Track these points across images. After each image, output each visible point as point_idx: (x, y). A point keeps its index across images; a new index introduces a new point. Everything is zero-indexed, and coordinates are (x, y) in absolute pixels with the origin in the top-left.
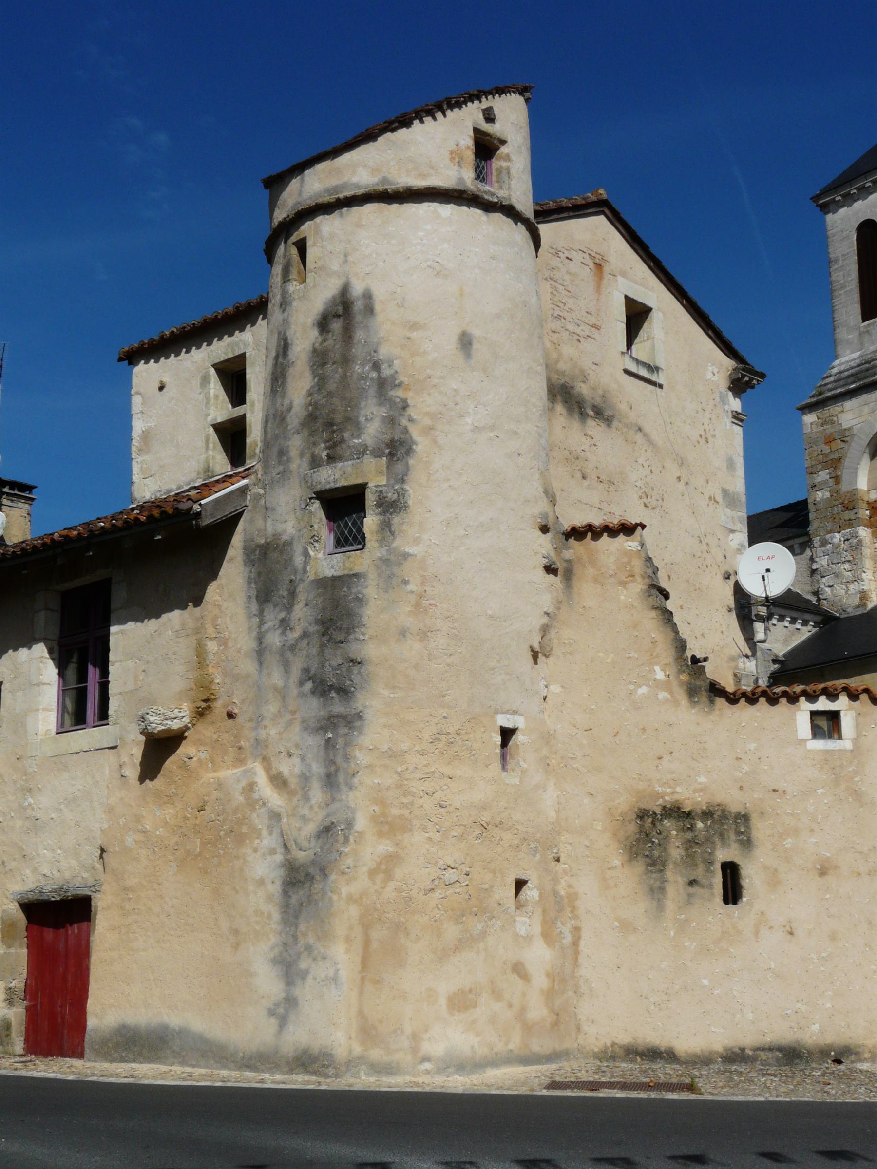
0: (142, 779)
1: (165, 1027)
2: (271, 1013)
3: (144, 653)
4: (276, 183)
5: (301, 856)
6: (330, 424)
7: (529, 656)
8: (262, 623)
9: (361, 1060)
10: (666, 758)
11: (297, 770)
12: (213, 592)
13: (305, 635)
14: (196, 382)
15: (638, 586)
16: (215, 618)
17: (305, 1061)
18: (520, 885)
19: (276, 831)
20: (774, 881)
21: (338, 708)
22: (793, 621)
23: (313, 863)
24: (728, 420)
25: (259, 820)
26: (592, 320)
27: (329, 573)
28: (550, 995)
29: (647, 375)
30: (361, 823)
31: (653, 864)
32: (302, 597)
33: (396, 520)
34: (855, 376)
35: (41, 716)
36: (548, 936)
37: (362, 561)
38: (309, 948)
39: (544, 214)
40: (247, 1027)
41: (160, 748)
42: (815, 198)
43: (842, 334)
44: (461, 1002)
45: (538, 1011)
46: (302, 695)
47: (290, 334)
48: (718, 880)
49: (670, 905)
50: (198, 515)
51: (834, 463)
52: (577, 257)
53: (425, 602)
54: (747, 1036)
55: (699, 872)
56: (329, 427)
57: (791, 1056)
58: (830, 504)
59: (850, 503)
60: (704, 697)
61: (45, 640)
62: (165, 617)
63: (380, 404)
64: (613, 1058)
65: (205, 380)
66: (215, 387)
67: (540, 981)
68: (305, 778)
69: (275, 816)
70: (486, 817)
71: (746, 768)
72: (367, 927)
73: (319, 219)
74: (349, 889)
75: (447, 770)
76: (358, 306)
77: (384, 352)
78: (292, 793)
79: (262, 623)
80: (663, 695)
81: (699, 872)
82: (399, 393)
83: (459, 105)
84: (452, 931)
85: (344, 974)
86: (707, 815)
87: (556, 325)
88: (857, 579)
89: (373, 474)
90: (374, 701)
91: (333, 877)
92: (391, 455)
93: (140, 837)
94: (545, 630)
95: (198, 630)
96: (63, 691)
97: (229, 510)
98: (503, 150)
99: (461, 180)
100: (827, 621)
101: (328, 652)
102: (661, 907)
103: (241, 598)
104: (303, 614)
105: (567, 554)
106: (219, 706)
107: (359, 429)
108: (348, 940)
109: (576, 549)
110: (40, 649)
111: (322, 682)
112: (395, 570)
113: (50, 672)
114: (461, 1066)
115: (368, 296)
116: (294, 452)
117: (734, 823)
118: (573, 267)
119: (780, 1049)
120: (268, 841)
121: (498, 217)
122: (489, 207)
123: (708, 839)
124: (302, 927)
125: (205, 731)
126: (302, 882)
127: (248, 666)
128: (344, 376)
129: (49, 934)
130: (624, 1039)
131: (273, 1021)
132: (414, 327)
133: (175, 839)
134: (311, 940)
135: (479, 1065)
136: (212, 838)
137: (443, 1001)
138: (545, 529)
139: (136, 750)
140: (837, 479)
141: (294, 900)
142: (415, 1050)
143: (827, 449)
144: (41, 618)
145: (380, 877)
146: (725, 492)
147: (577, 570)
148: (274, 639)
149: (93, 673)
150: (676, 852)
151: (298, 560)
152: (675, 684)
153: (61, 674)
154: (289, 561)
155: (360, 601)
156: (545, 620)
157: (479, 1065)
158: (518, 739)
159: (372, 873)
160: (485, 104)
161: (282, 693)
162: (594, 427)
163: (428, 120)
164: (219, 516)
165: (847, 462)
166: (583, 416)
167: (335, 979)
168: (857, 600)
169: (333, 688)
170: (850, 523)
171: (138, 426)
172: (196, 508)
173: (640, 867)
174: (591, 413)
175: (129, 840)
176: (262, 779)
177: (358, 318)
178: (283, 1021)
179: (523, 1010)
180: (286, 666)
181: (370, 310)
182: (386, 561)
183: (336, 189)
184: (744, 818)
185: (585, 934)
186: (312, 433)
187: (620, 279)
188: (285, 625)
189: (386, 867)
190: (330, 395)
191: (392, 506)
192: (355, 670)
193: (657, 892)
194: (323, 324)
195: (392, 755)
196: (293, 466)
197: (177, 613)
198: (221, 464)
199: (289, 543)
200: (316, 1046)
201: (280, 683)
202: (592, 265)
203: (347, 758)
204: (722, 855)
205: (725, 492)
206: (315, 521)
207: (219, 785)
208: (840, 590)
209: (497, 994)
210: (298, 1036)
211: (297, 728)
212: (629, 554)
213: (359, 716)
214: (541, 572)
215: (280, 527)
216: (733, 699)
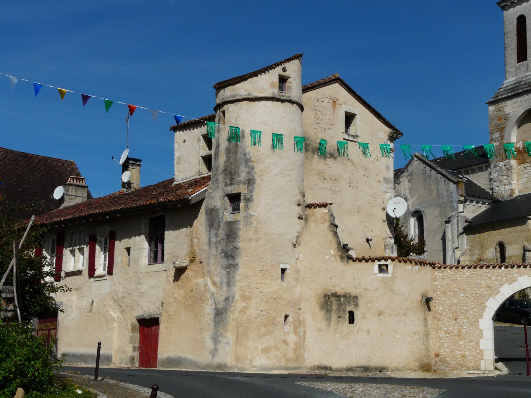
0: (174, 281)
1: (180, 358)
2: (211, 353)
3: (175, 240)
5: (220, 307)
6: (231, 173)
7: (292, 246)
8: (210, 234)
9: (235, 366)
10: (333, 278)
11: (219, 280)
12: (196, 223)
13: (222, 239)
14: (196, 140)
15: (327, 224)
16: (196, 232)
18: (286, 317)
19: (213, 298)
20: (364, 317)
21: (231, 262)
22: (478, 203)
23: (223, 308)
25: (208, 295)
26: (331, 122)
27: (230, 220)
28: (295, 350)
30: (237, 297)
31: (328, 311)
32: (222, 227)
33: (249, 204)
34: (512, 89)
35: (143, 259)
36: (296, 332)
37: (240, 216)
38: (221, 334)
41: (180, 272)
42: (499, 3)
43: (509, 68)
44: (266, 351)
45: (291, 355)
46: (221, 257)
47: (220, 141)
48: (347, 316)
49: (332, 324)
50: (191, 200)
51: (501, 130)
52: (326, 100)
53: (258, 230)
54: (353, 363)
55: (341, 314)
56: (231, 174)
60: (345, 259)
62: (181, 230)
63: (246, 167)
64: (314, 369)
65: (199, 140)
66: (203, 143)
67: (292, 346)
68: (221, 283)
69: (213, 294)
70: (275, 296)
72: (238, 328)
73: (229, 105)
74: (233, 317)
75: (263, 282)
78: (218, 287)
79: (210, 234)
80: (333, 259)
81: (341, 314)
82: (251, 164)
83: (274, 68)
84: (263, 330)
85: (231, 342)
86: (345, 296)
88: (509, 184)
89: (243, 189)
90: (241, 260)
91: (228, 313)
92: (249, 184)
93: (173, 299)
94: (298, 237)
95: (191, 235)
96: (150, 251)
97: (200, 198)
98: (289, 80)
99: (273, 93)
100: (495, 203)
101: (229, 245)
102: (330, 324)
103: (204, 226)
104: (222, 232)
105: (306, 213)
106: (197, 259)
107: (239, 175)
108: (232, 331)
109: (309, 211)
110: (143, 237)
111: (227, 254)
112: (249, 220)
113: (146, 245)
114: (264, 369)
116: (220, 180)
117: (353, 299)
118: (323, 104)
119: (363, 367)
120: (211, 302)
122: (282, 101)
123: (345, 304)
124: (220, 328)
125: (193, 267)
126: (220, 314)
127: (206, 247)
128: (235, 158)
129: (146, 329)
131: (211, 355)
133: (184, 300)
134: (222, 331)
136: (195, 300)
137: (260, 350)
138: (299, 205)
139: (172, 272)
140: (502, 137)
141: (217, 320)
142: (251, 364)
143: (498, 123)
144: (143, 226)
145: (242, 313)
146: (385, 178)
147: (309, 218)
148: (214, 239)
149: (159, 246)
150: (335, 307)
151: (221, 215)
152: (337, 255)
153: (150, 245)
154: (218, 215)
155: (238, 229)
156: (298, 234)
158: (287, 272)
159: (240, 312)
160: (283, 66)
161: (215, 256)
162: (330, 161)
163: (263, 74)
164: (197, 200)
165: (507, 129)
167: (228, 343)
169: (230, 255)
171: (177, 154)
172: (190, 198)
173: (324, 312)
174: (329, 156)
175: (170, 300)
178: (214, 355)
179: (286, 354)
180: (217, 248)
182: (246, 217)
183: (234, 96)
184: (356, 297)
185: (307, 332)
186: (226, 175)
187: (343, 105)
188: (217, 235)
189: (244, 310)
190: (231, 163)
191: (248, 200)
192: (236, 250)
193: (329, 319)
194: (230, 139)
195: (247, 277)
196: (220, 185)
197: (185, 229)
198: (204, 169)
199: (218, 209)
200: (223, 362)
201: (215, 253)
202: (331, 102)
203: (233, 277)
204: (349, 309)
205: (385, 178)
206: (226, 203)
207: (197, 284)
208: (502, 188)
209: (277, 349)
210: (217, 360)
211: (219, 267)
212: (324, 213)
213: (237, 265)
214: (297, 219)
215: (216, 204)
216: (354, 261)
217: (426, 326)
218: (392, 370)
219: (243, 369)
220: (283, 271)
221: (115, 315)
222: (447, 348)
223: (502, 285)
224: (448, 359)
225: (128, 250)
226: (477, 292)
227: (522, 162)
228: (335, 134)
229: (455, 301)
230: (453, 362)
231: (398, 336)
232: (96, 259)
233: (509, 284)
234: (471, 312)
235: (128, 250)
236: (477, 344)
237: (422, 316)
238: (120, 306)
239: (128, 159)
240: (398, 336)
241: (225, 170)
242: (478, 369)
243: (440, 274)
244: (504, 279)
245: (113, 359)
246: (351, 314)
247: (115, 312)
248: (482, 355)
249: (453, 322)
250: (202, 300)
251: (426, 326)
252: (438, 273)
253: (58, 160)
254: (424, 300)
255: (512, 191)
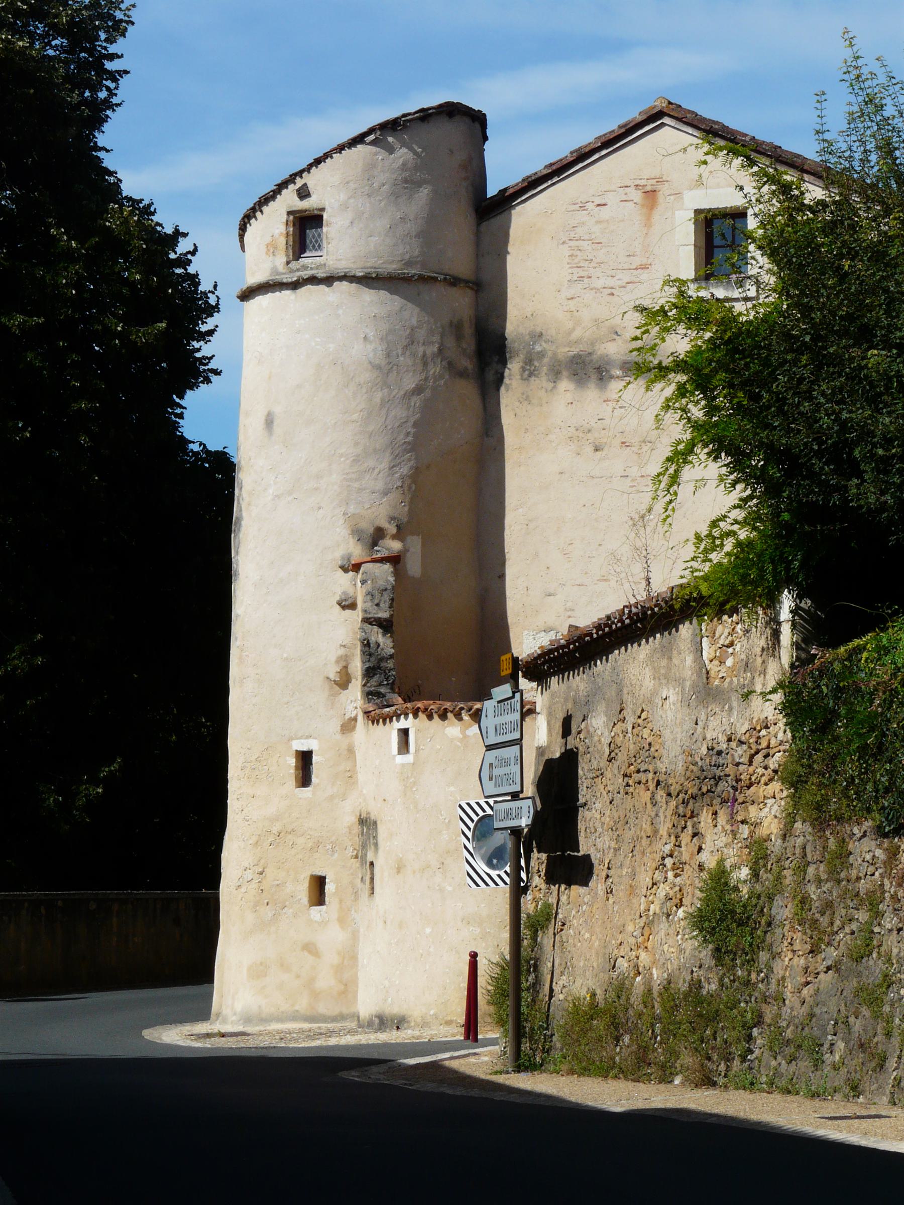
26: (637, 261)
28: (339, 970)
45: (326, 981)
87: (577, 289)
99: (275, 271)
122: (295, 285)
174: (619, 373)
202: (637, 196)
209: (284, 966)
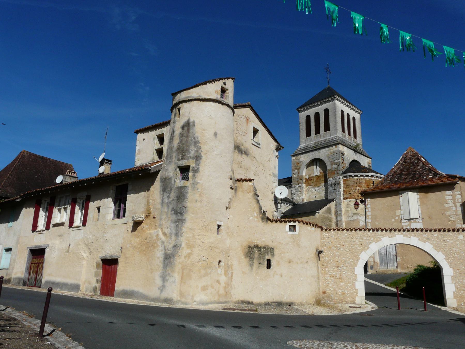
0: (132, 232)
1: (133, 291)
2: (159, 289)
3: (135, 202)
4: (174, 95)
5: (168, 252)
6: (183, 151)
7: (225, 208)
8: (163, 196)
9: (180, 301)
10: (256, 234)
11: (169, 232)
12: (152, 188)
13: (173, 200)
14: (152, 139)
15: (252, 194)
16: (152, 194)
17: (166, 300)
18: (220, 262)
19: (163, 246)
20: (278, 264)
21: (180, 217)
22: (287, 204)
23: (171, 254)
24: (275, 157)
25: (159, 243)
27: (180, 186)
28: (225, 288)
29: (257, 145)
30: (183, 245)
31: (251, 258)
32: (173, 191)
33: (196, 174)
34: (304, 150)
35: (109, 215)
36: (225, 274)
37: (188, 183)
38: (169, 274)
39: (236, 107)
40: (153, 292)
41: (137, 224)
42: (297, 109)
43: (301, 140)
44: (204, 289)
45: (222, 292)
46: (171, 214)
47: (175, 129)
48: (266, 263)
49: (254, 268)
50: (150, 170)
51: (298, 169)
52: (243, 117)
53: (202, 194)
54: (270, 299)
55: (261, 261)
56: (182, 151)
57: (279, 304)
58: (297, 178)
59: (301, 178)
60: (265, 220)
61: (111, 197)
62: (140, 193)
63: (195, 147)
64: (239, 303)
65: (154, 139)
66: (157, 141)
67: (223, 284)
68: (171, 234)
69: (163, 242)
70: (213, 245)
71: (274, 237)
72: (183, 270)
73: (184, 104)
74: (179, 261)
75: (205, 234)
76: (191, 124)
77: (196, 135)
78: (167, 237)
79: (163, 196)
80: (256, 219)
81: (261, 261)
82: (199, 145)
83: (218, 81)
84: (203, 272)
85: (177, 280)
86: (264, 248)
87: (237, 132)
88: (302, 196)
89: (192, 163)
90: (188, 216)
91: (176, 257)
92: (196, 159)
93: (131, 245)
94: (229, 202)
96: (115, 210)
97: (157, 169)
98: (227, 91)
99: (217, 97)
100: (294, 205)
101: (178, 204)
102: (252, 269)
103: (159, 190)
105: (236, 185)
106: (152, 215)
108: (178, 272)
109: (238, 184)
110: (110, 199)
111: (177, 211)
112: (196, 186)
113: (112, 205)
114: (203, 304)
115: (194, 122)
116: (174, 157)
117: (270, 250)
118: (242, 119)
119: (277, 303)
120: (161, 248)
121: (225, 106)
122: (223, 104)
123: (264, 253)
124: (168, 269)
125: (148, 221)
126: (168, 258)
127: (159, 206)
128: (187, 140)
129: (107, 267)
130: (242, 299)
131: (159, 291)
132: (204, 130)
133: (139, 246)
134: (170, 272)
135: (208, 303)
137: (200, 288)
138: (231, 179)
139: (131, 224)
140: (299, 172)
141: (166, 262)
142: (192, 299)
143: (297, 166)
144: (111, 191)
145: (187, 258)
146: (273, 173)
147: (238, 189)
148: (166, 200)
149: (122, 206)
150: (256, 256)
151: (173, 182)
152: (259, 217)
153: (115, 205)
154: (171, 182)
155: (187, 193)
156: (230, 200)
157: (208, 303)
158: (221, 227)
159: (185, 257)
160: (224, 81)
161: (167, 213)
163: (211, 83)
164: (155, 170)
165: (301, 169)
166: (242, 153)
167: (175, 282)
168: (301, 201)
170: (301, 183)
171: (138, 148)
172: (150, 168)
173: (248, 259)
175: (128, 246)
176: (160, 233)
177: (191, 127)
178: (162, 291)
179: (218, 291)
180: (168, 207)
181: (194, 125)
182: (194, 184)
183: (188, 97)
184: (273, 249)
185: (234, 274)
186: (178, 153)
188: (169, 197)
189: (188, 256)
190: (183, 144)
192: (184, 209)
193: (252, 265)
194: (183, 128)
195: (192, 229)
196: (173, 160)
197: (143, 192)
198: (157, 158)
199: (171, 178)
200: (169, 297)
201: (166, 211)
203: (181, 229)
204: (267, 257)
205: (273, 173)
206: (177, 173)
207: (150, 234)
208: (298, 198)
209: (213, 287)
210: (165, 295)
211: (170, 222)
212: (250, 186)
213: (185, 220)
214: (230, 189)
215: (169, 174)
216: (272, 221)
217: (318, 271)
218: (298, 305)
219: (186, 303)
220: (219, 226)
221: (85, 255)
222: (332, 287)
223: (371, 243)
224: (332, 296)
225: (99, 209)
226: (353, 247)
227: (308, 185)
228: (247, 141)
229: (337, 254)
230: (336, 298)
231: (302, 279)
232: (75, 215)
233: (376, 242)
234: (349, 262)
235: (99, 209)
236: (353, 285)
237: (316, 264)
238: (89, 249)
239: (104, 159)
240: (302, 279)
241: (178, 149)
242: (354, 303)
243: (327, 235)
244: (372, 239)
245: (81, 288)
246: (269, 261)
247: (85, 253)
248: (357, 293)
249: (336, 269)
250: (154, 246)
251: (318, 271)
252: (325, 234)
253: (62, 163)
254: (317, 253)
255: (303, 200)
